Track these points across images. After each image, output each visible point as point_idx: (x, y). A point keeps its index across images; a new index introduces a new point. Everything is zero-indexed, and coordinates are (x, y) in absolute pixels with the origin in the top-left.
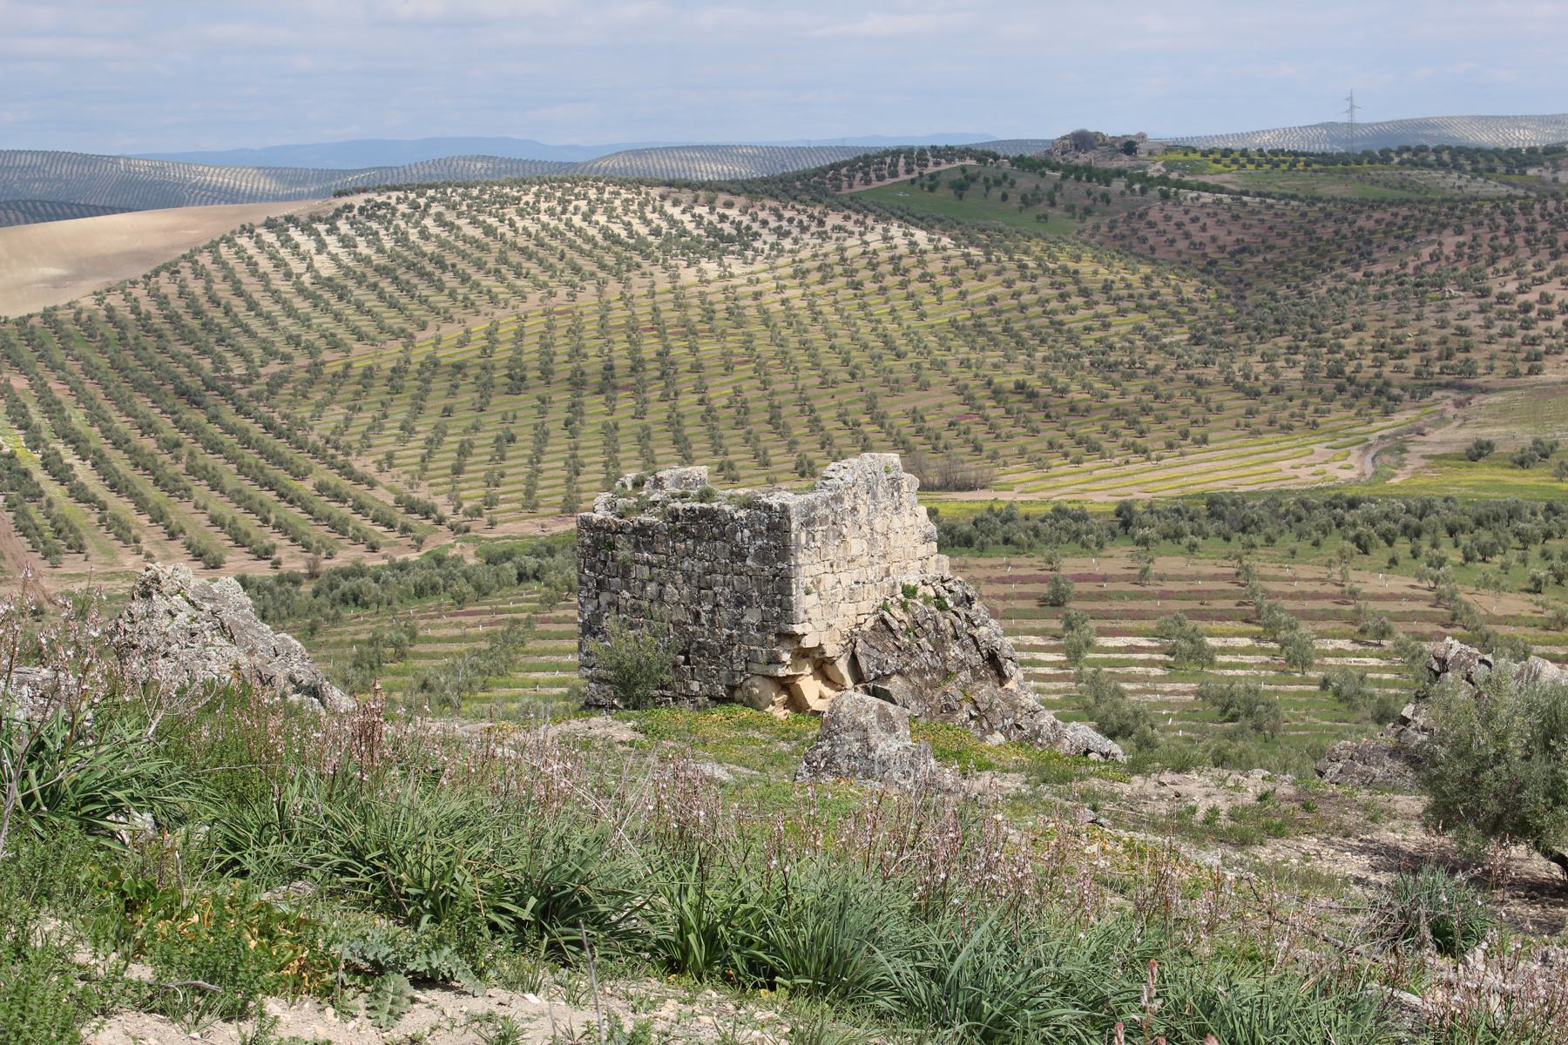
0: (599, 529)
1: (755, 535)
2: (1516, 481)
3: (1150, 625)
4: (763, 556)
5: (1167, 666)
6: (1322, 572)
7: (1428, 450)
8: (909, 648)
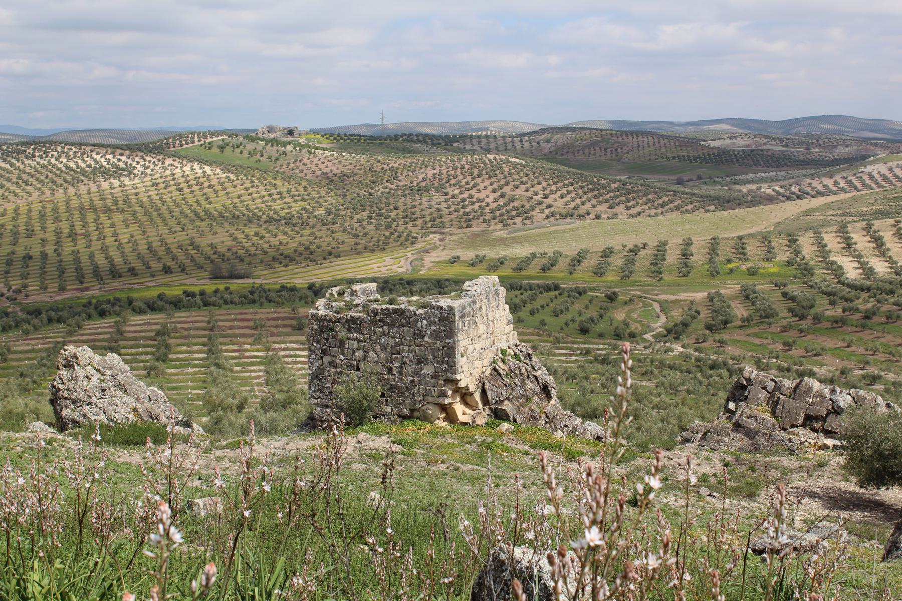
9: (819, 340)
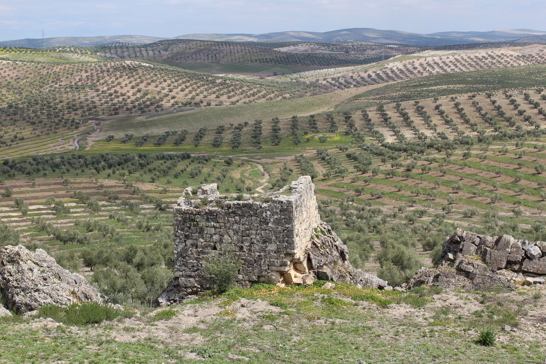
0: (186, 213)
1: (273, 214)
2: (124, 147)
4: (278, 222)
5: (54, 214)
6: (88, 180)
7: (94, 139)
8: (325, 254)
9: (379, 187)
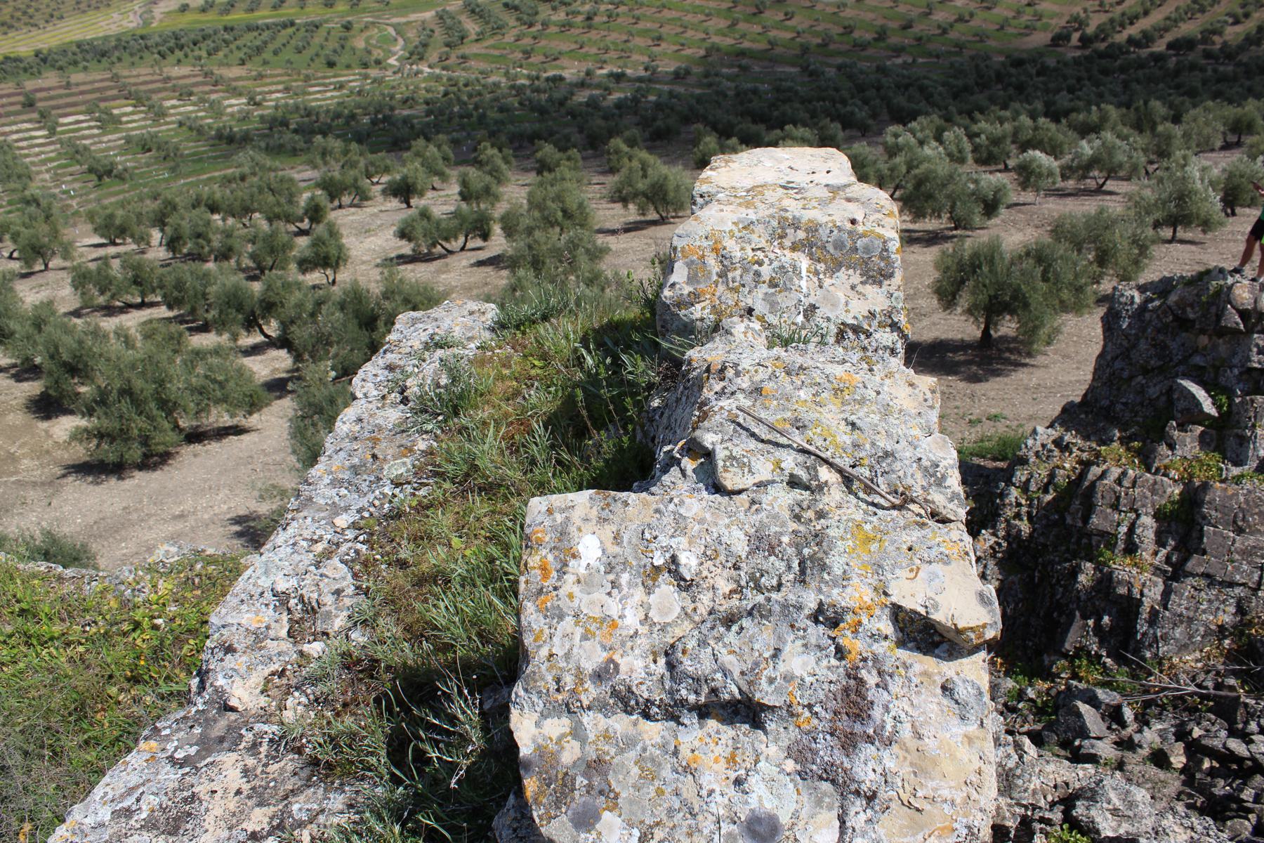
3: (83, 108)
5: (98, 127)
6: (150, 70)
9: (553, 44)
